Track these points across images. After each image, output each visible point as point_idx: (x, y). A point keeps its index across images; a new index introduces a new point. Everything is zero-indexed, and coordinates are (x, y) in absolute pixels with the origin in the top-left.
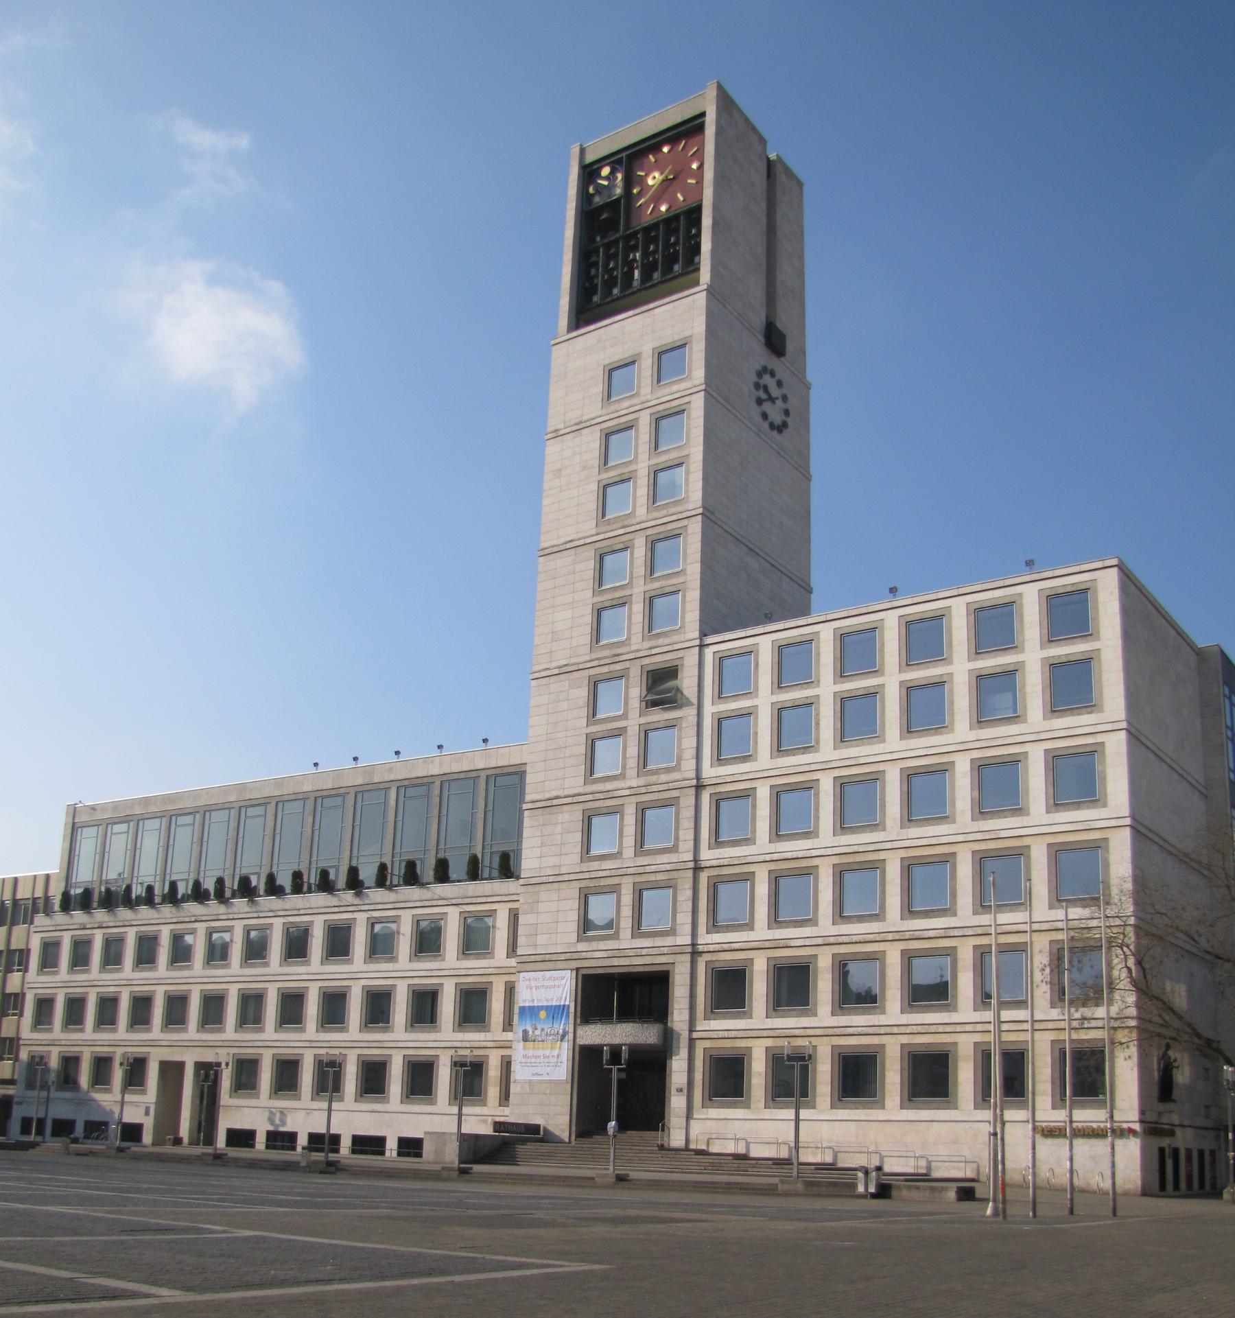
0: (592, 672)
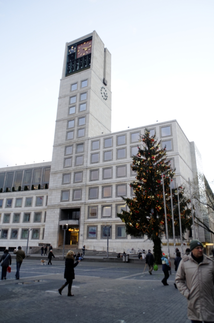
0: (66, 145)
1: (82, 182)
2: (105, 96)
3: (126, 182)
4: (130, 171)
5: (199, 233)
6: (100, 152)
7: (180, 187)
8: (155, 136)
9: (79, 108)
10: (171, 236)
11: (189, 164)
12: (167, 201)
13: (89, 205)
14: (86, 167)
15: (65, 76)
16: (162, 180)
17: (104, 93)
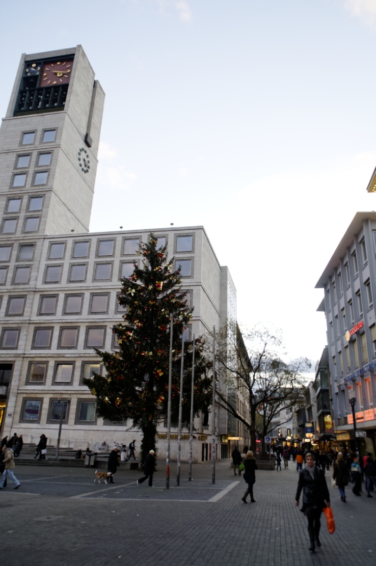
1: (21, 315)
2: (85, 166)
3: (105, 324)
4: (116, 305)
5: (219, 418)
6: (63, 264)
7: (198, 341)
8: (165, 248)
9: (34, 178)
10: (174, 422)
11: (216, 303)
12: (173, 362)
13: (30, 359)
14: (34, 290)
15: (12, 115)
16: (170, 326)
17: (84, 160)
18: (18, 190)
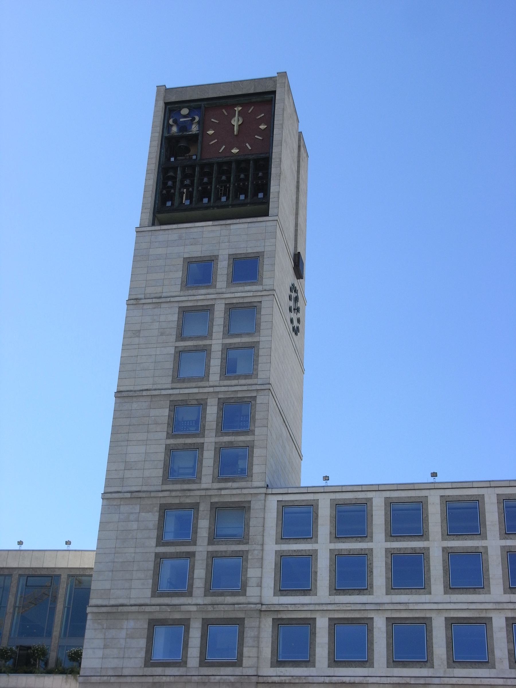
0: (163, 501)
1: (238, 663)
18: (194, 384)
